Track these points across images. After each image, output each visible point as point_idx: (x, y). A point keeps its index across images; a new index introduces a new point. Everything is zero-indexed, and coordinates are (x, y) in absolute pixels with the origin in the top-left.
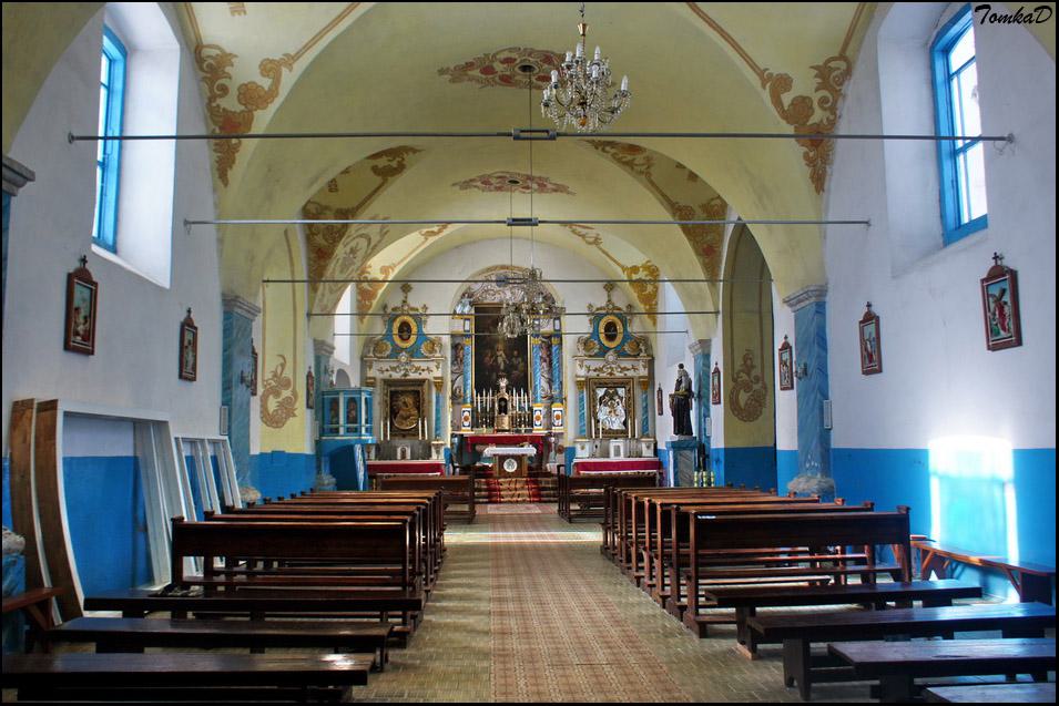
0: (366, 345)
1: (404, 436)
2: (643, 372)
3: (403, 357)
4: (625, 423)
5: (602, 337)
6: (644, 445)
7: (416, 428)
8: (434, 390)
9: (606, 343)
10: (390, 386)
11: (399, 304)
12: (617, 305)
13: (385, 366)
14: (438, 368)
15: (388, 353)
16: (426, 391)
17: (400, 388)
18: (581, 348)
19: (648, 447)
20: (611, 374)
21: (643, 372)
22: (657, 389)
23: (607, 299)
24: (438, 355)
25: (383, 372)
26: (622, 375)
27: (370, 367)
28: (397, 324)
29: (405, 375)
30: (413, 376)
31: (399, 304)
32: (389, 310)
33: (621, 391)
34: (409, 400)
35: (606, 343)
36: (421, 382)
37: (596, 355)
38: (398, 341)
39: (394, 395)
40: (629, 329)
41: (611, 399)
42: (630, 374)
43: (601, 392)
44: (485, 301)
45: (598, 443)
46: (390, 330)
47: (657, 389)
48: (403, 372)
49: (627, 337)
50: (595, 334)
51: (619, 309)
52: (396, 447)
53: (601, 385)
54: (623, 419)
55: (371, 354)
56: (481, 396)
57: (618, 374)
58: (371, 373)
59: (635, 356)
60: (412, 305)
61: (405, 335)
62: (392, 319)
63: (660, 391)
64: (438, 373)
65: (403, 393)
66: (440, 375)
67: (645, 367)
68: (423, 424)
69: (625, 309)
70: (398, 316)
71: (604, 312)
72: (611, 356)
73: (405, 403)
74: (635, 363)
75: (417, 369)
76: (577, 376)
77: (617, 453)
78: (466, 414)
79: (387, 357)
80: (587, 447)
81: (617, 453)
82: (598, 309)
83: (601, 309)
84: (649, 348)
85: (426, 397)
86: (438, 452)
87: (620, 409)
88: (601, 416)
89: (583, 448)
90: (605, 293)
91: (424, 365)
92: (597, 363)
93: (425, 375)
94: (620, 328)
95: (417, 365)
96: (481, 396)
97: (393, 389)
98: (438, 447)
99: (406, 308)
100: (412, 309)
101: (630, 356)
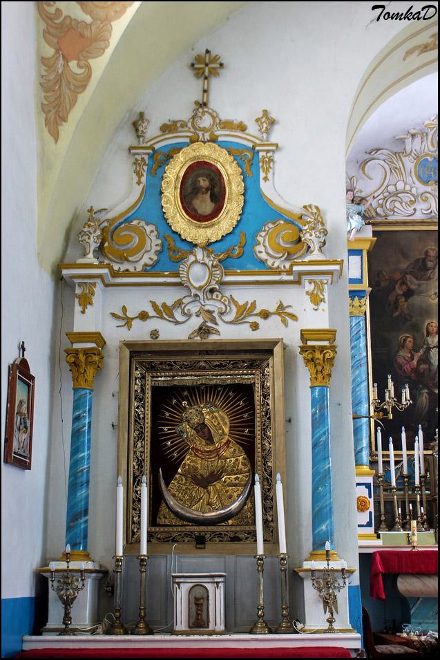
0: (73, 236)
1: (200, 541)
3: (197, 274)
7: (244, 516)
8: (304, 376)
10: (152, 368)
11: (184, 114)
13: (137, 301)
14: (316, 300)
15: (146, 259)
16: (277, 386)
17: (188, 379)
24: (316, 255)
25: (128, 322)
27: (86, 301)
28: (175, 171)
29: (204, 331)
30: (228, 332)
31: (184, 114)
32: (152, 130)
34: (218, 418)
36: (260, 353)
38: (181, 223)
39: (164, 399)
44: (392, 218)
46: (154, 191)
48: (196, 322)
52: (175, 581)
55: (91, 258)
56: (398, 447)
58: (84, 321)
60: (225, 115)
61: (204, 205)
62: (161, 159)
64: (316, 318)
65: (197, 393)
66: (324, 325)
68: (268, 498)
70: (177, 149)
73: (202, 429)
75: (245, 312)
78: (363, 492)
79: (146, 272)
85: (276, 403)
86: (329, 603)
91: (266, 299)
93: (269, 330)
95: (243, 296)
96: (398, 447)
97: (162, 380)
98: (326, 580)
99: (206, 122)
100: (227, 125)
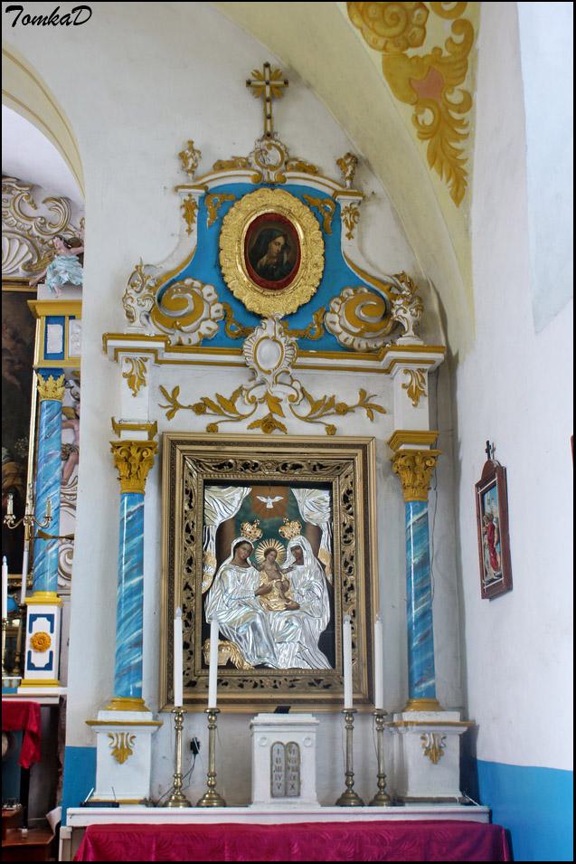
2: (412, 416)
4: (328, 642)
5: (237, 273)
6: (413, 746)
9: (252, 297)
12: (303, 153)
18: (142, 305)
19: (435, 754)
20: (269, 424)
21: (412, 416)
22: (472, 471)
23: (259, 133)
26: (316, 431)
33: (313, 505)
35: (252, 297)
37: (206, 343)
40: (348, 247)
41: (272, 533)
42: (352, 426)
43: (224, 504)
45: (198, 728)
47: (472, 471)
49: (336, 272)
50: (206, 260)
51: (313, 170)
53: (222, 471)
54: (319, 625)
57: (297, 427)
59: (374, 354)
63: (494, 477)
67: (414, 395)
69: (332, 171)
71: (244, 177)
72: (267, 349)
74: (374, 384)
76: (118, 427)
77: (287, 784)
80: (142, 746)
81: (287, 784)
82: (220, 166)
83: (233, 164)
84: (433, 322)
87: (308, 579)
88: (221, 614)
89: (121, 754)
90: (255, 107)
92: (218, 381)
94: (307, 230)
101: (349, 350)
